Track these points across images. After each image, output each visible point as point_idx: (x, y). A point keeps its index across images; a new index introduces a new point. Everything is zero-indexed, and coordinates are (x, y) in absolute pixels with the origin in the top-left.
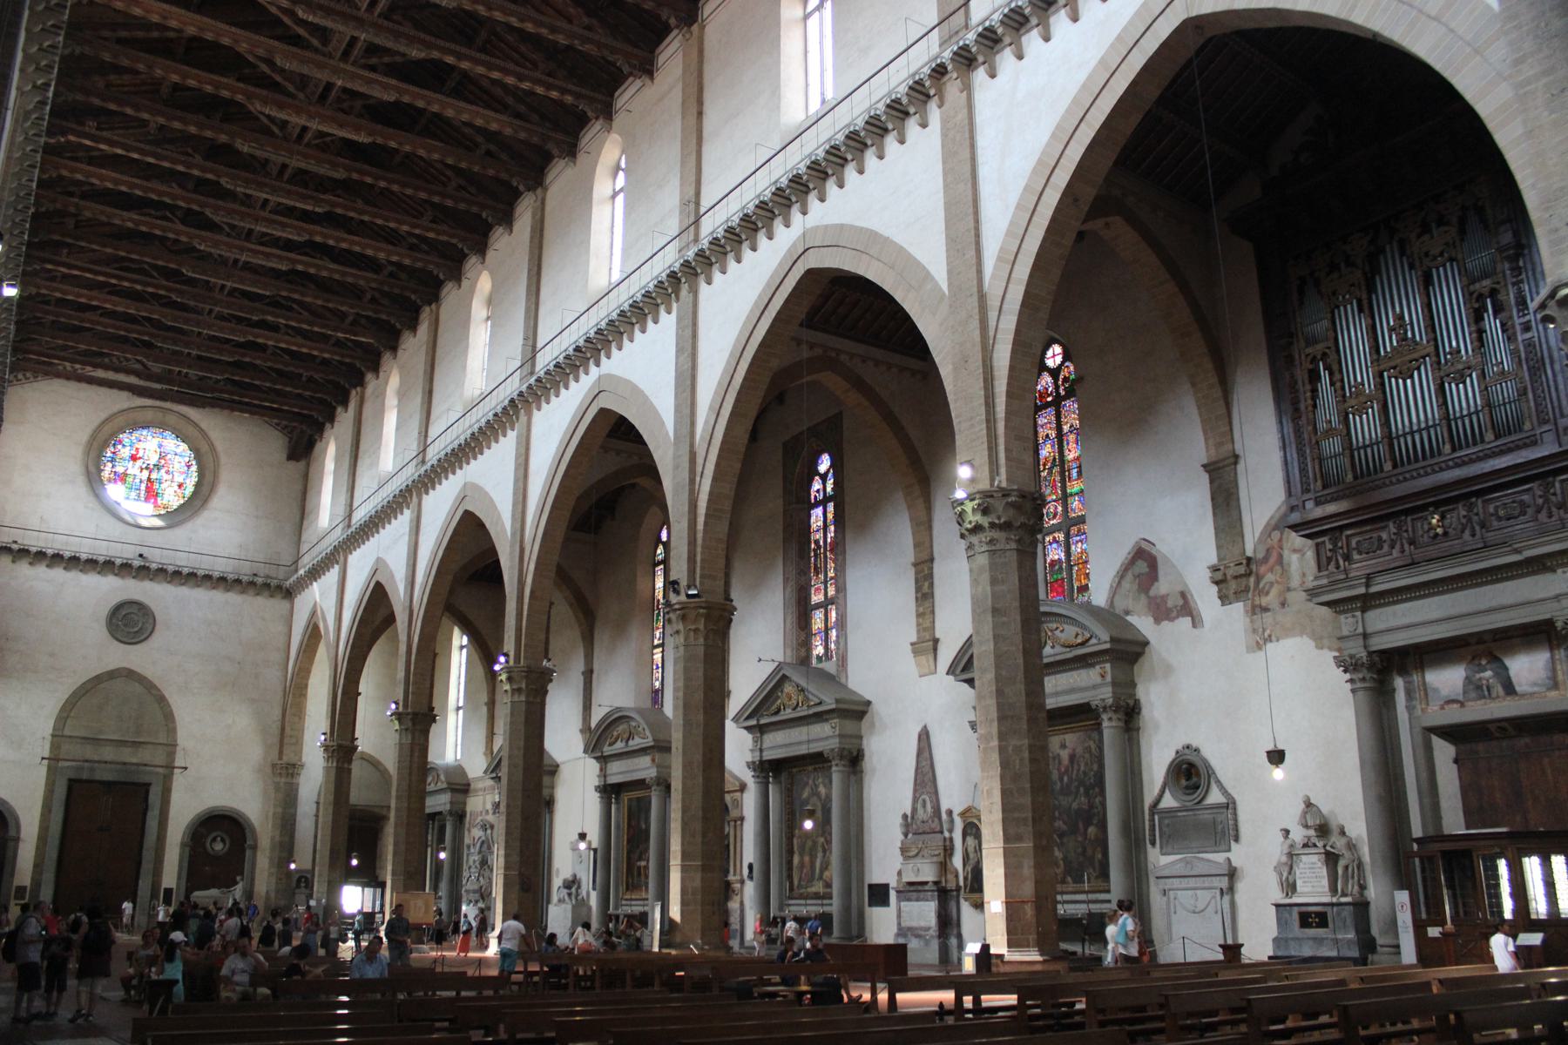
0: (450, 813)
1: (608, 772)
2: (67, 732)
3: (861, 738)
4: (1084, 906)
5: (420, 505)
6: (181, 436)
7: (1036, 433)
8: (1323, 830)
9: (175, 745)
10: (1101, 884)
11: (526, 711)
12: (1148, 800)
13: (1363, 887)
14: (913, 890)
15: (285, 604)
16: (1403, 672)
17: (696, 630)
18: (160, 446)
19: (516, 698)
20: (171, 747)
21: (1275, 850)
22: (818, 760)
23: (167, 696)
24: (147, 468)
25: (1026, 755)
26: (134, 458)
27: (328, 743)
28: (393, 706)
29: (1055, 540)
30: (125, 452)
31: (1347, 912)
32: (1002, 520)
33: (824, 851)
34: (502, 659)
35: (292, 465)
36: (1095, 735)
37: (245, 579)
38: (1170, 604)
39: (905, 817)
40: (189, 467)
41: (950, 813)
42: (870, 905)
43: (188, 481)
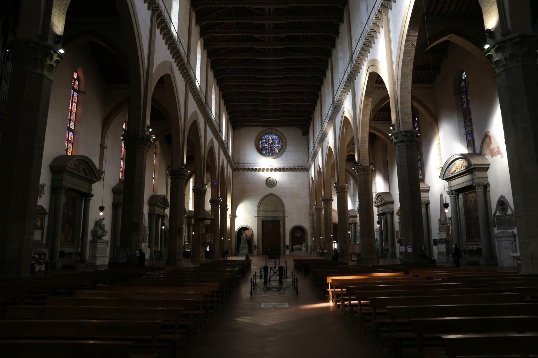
2: (260, 210)
4: (477, 246)
5: (322, 145)
7: (462, 101)
9: (285, 211)
15: (307, 173)
17: (361, 174)
18: (272, 138)
20: (284, 211)
23: (281, 199)
26: (266, 142)
29: (469, 134)
32: (401, 140)
37: (296, 168)
38: (495, 151)
40: (279, 142)
42: (434, 246)
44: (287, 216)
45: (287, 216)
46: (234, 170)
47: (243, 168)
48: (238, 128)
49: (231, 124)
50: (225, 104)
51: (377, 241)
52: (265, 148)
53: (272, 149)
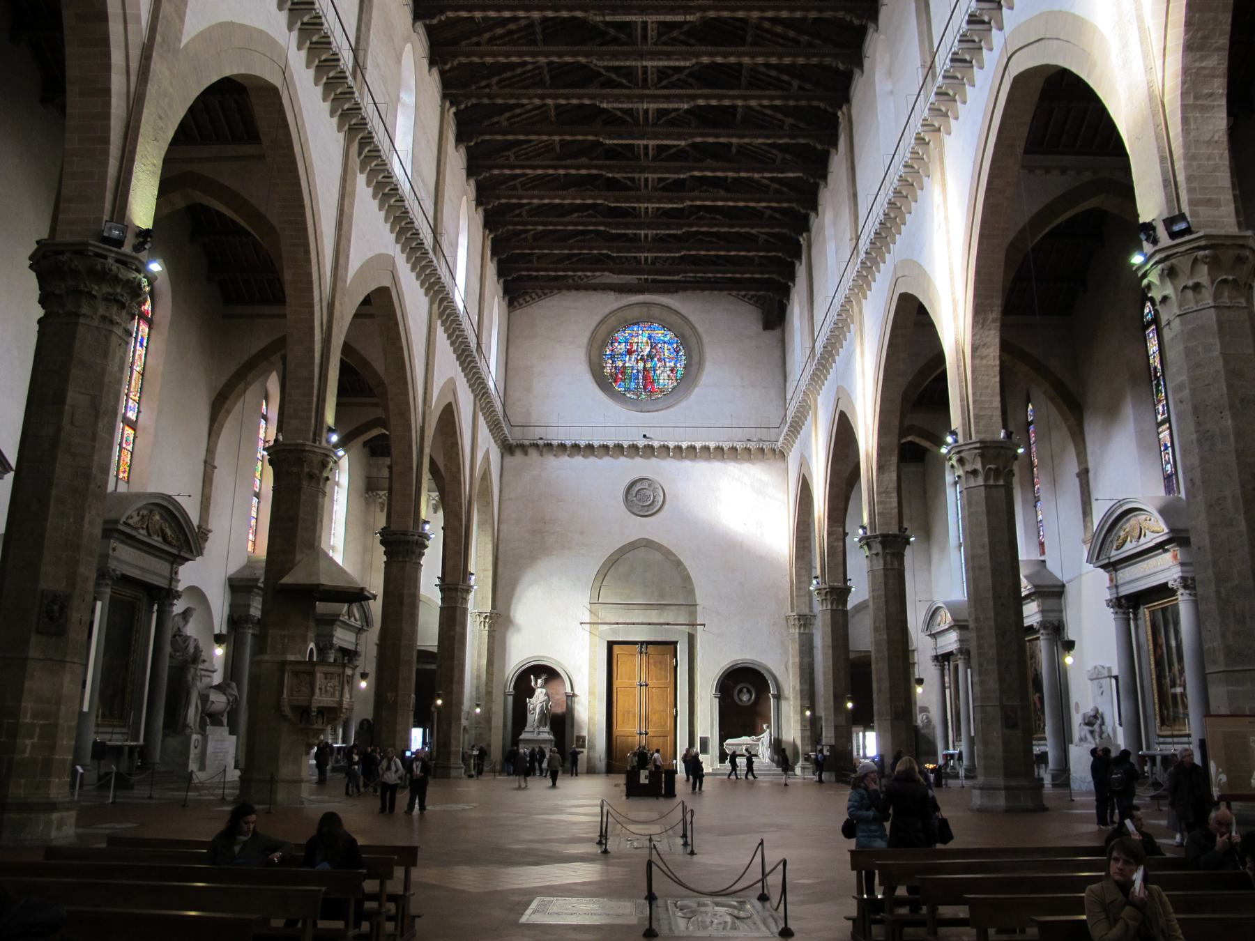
0: (960, 651)
1: (1120, 582)
6: (666, 326)
11: (987, 498)
17: (1197, 287)
18: (650, 337)
19: (972, 483)
24: (642, 359)
26: (629, 352)
27: (821, 586)
28: (861, 531)
30: (622, 348)
34: (949, 439)
35: (768, 334)
40: (677, 352)
43: (678, 365)
44: (704, 625)
45: (704, 625)
46: (508, 448)
47: (540, 442)
48: (528, 298)
49: (501, 273)
50: (471, 171)
51: (1099, 722)
52: (623, 373)
53: (648, 379)
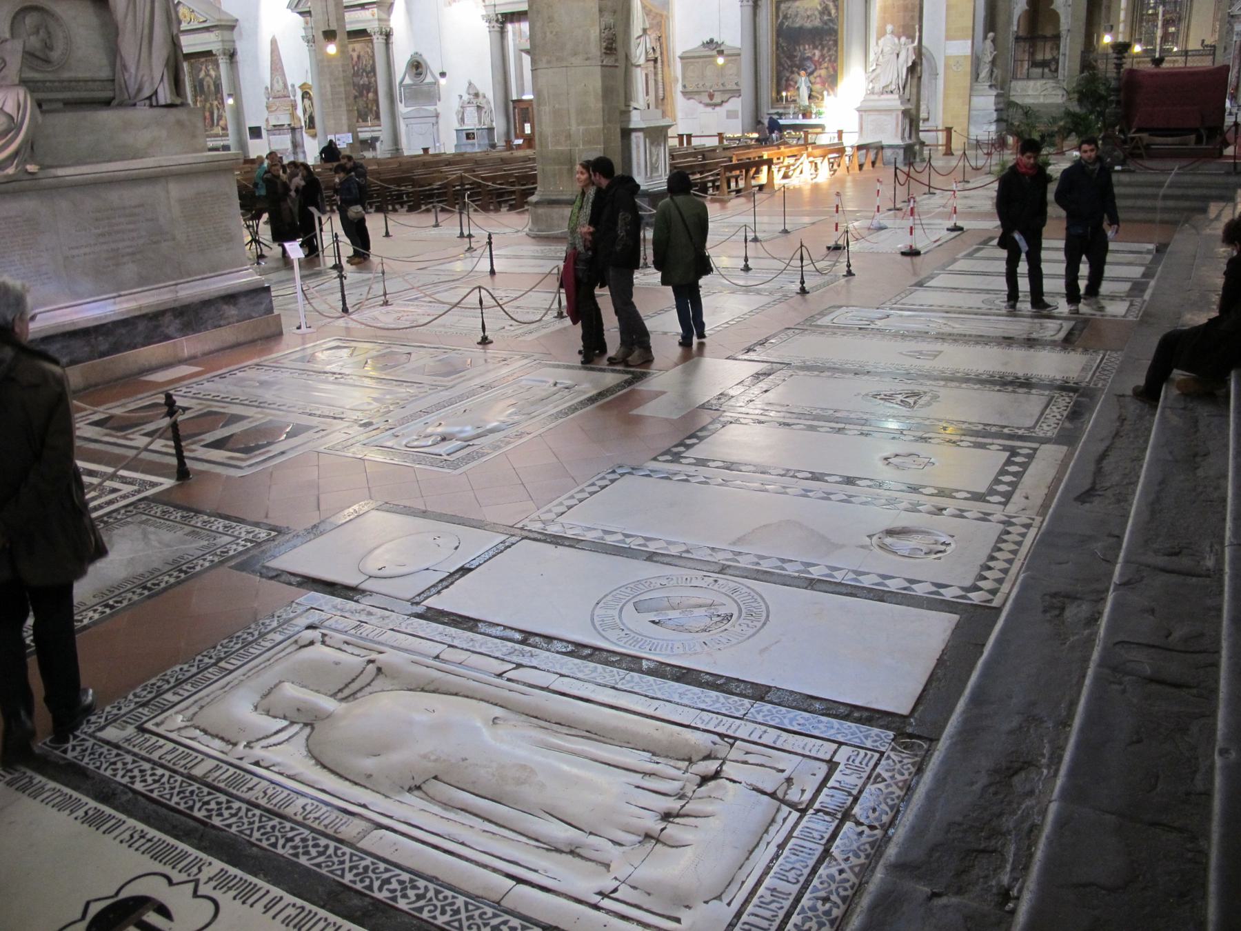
3: (234, 41)
8: (477, 95)
10: (376, 122)
12: (398, 81)
13: (492, 121)
14: (278, 128)
16: (512, 22)
21: (455, 105)
22: (208, 53)
25: (341, 69)
31: (485, 132)
33: (218, 109)
36: (370, 45)
39: (267, 88)
41: (293, 86)
